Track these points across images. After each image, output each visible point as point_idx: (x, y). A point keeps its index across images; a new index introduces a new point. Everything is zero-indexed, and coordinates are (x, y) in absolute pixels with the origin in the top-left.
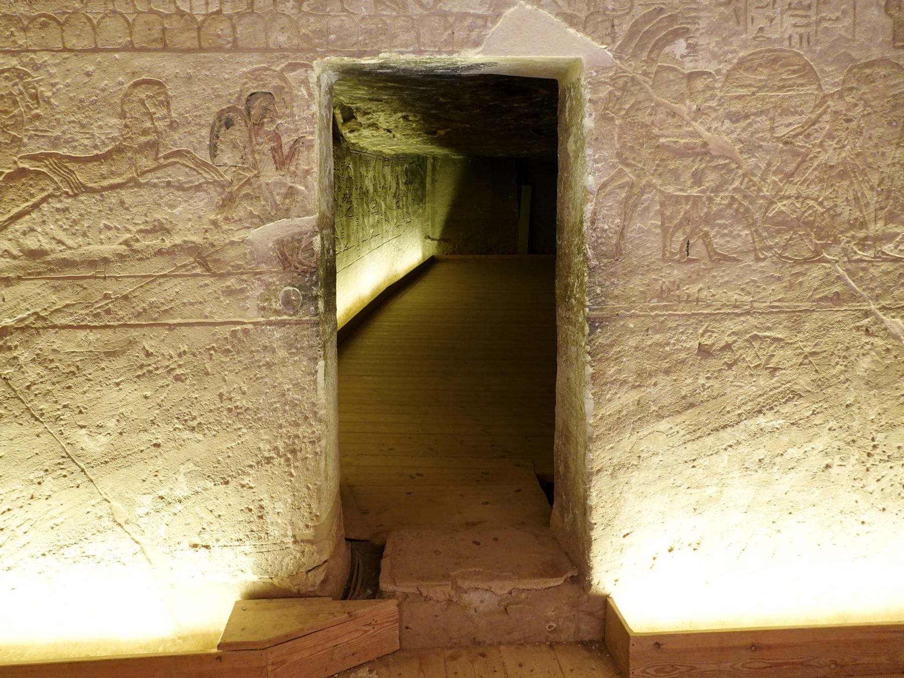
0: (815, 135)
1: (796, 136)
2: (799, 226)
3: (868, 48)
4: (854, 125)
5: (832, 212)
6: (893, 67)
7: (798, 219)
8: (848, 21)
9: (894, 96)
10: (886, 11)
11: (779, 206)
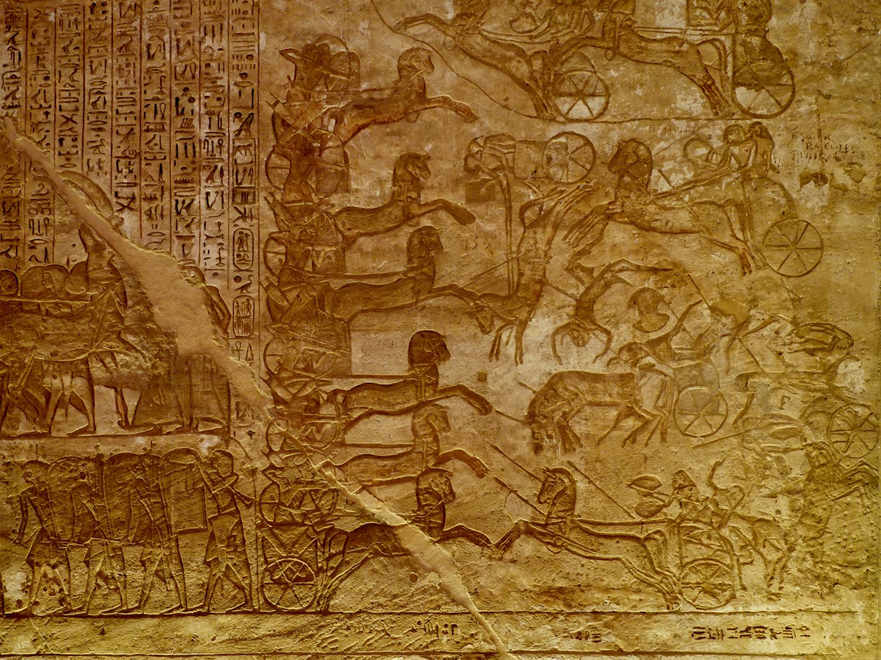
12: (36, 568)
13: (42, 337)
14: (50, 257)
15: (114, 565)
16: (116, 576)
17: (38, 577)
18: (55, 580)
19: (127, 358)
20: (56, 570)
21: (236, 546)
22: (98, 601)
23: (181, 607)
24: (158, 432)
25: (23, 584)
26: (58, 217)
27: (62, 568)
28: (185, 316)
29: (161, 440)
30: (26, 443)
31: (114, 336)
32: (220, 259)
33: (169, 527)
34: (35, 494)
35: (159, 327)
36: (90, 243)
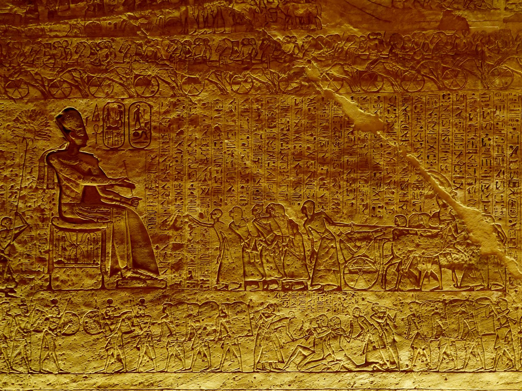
12: (415, 350)
13: (418, 245)
14: (422, 209)
15: (452, 349)
16: (453, 354)
17: (416, 354)
18: (424, 355)
19: (457, 256)
20: (424, 351)
21: (509, 342)
22: (444, 365)
23: (483, 368)
24: (472, 290)
25: (409, 357)
26: (426, 192)
27: (427, 350)
28: (485, 237)
29: (474, 293)
30: (411, 294)
31: (452, 246)
32: (502, 212)
33: (477, 332)
34: (415, 317)
35: (472, 242)
36: (441, 203)
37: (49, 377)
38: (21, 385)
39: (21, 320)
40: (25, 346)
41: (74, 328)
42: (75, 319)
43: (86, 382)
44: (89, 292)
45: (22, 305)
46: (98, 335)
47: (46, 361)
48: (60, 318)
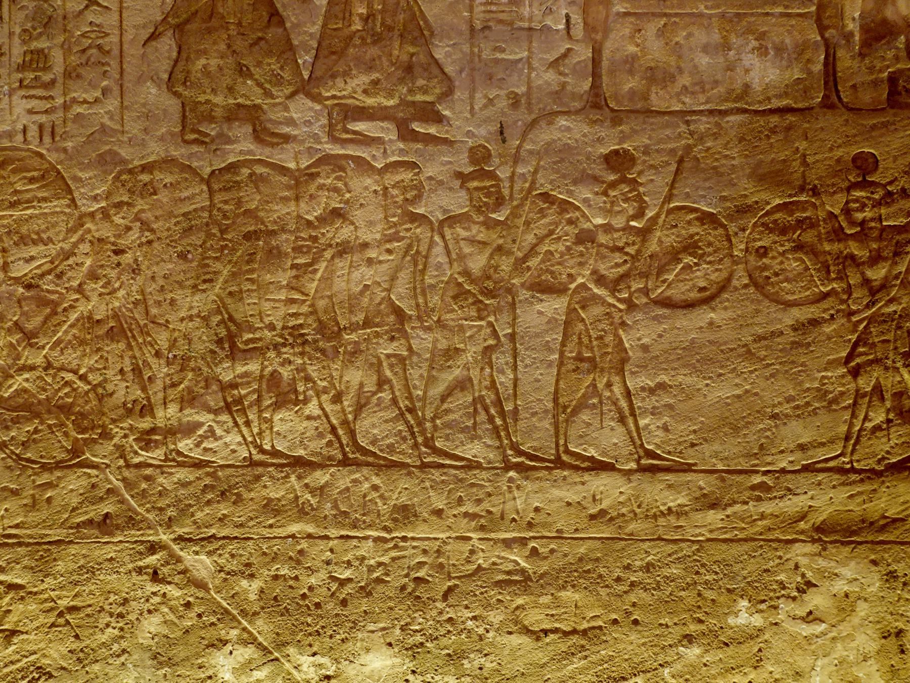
0: (70, 274)
1: (42, 275)
2: (49, 412)
3: (143, 144)
4: (127, 258)
5: (100, 390)
6: (182, 171)
7: (48, 399)
8: (112, 104)
9: (184, 215)
10: (169, 89)
11: (19, 381)
37: (600, 483)
38: (474, 516)
39: (471, 241)
40: (488, 350)
41: (705, 275)
42: (714, 235)
43: (768, 507)
44: (774, 120)
45: (471, 177)
46: (813, 308)
47: (585, 416)
48: (644, 233)
